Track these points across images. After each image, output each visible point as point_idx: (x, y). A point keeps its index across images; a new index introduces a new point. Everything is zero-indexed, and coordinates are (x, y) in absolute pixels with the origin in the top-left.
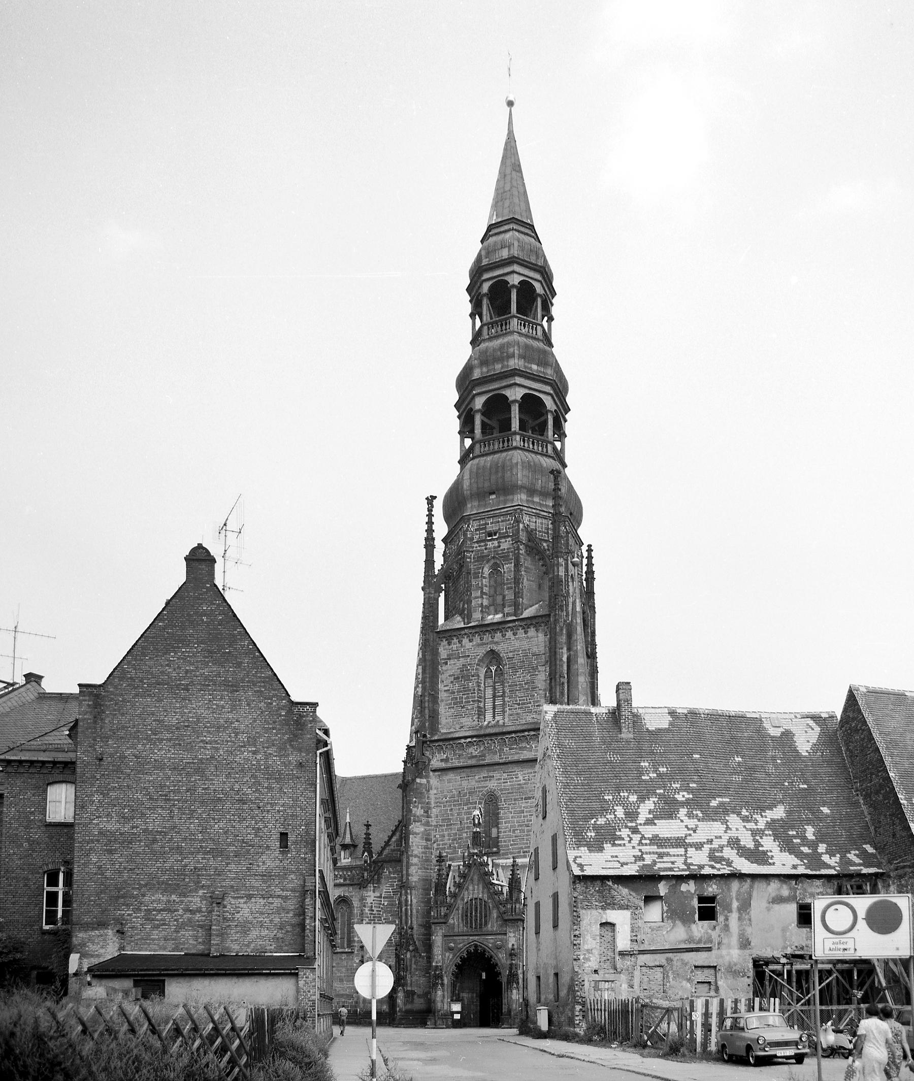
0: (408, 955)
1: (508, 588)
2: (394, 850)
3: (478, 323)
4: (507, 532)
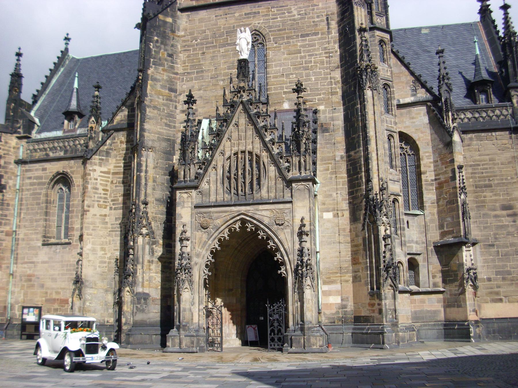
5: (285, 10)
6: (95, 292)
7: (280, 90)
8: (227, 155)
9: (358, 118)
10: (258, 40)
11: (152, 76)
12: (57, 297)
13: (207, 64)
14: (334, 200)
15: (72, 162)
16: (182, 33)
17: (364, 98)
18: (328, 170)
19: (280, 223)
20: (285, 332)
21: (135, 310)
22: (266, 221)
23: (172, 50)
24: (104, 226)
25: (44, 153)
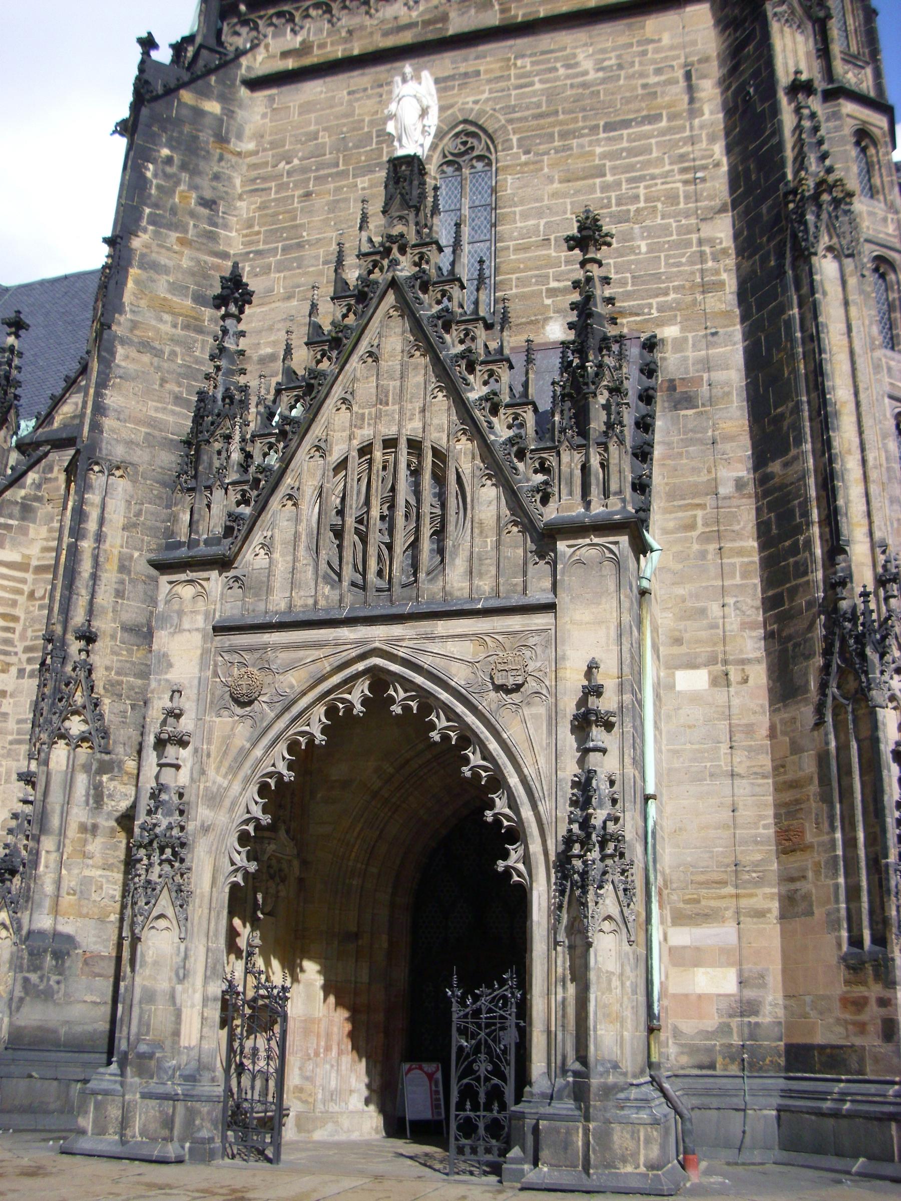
5: (557, 60)
7: (537, 283)
8: (335, 456)
9: (792, 348)
10: (472, 148)
11: (143, 255)
14: (714, 626)
16: (251, 146)
17: (812, 282)
18: (692, 527)
19: (510, 682)
20: (518, 1101)
21: (18, 993)
22: (459, 676)
23: (214, 188)
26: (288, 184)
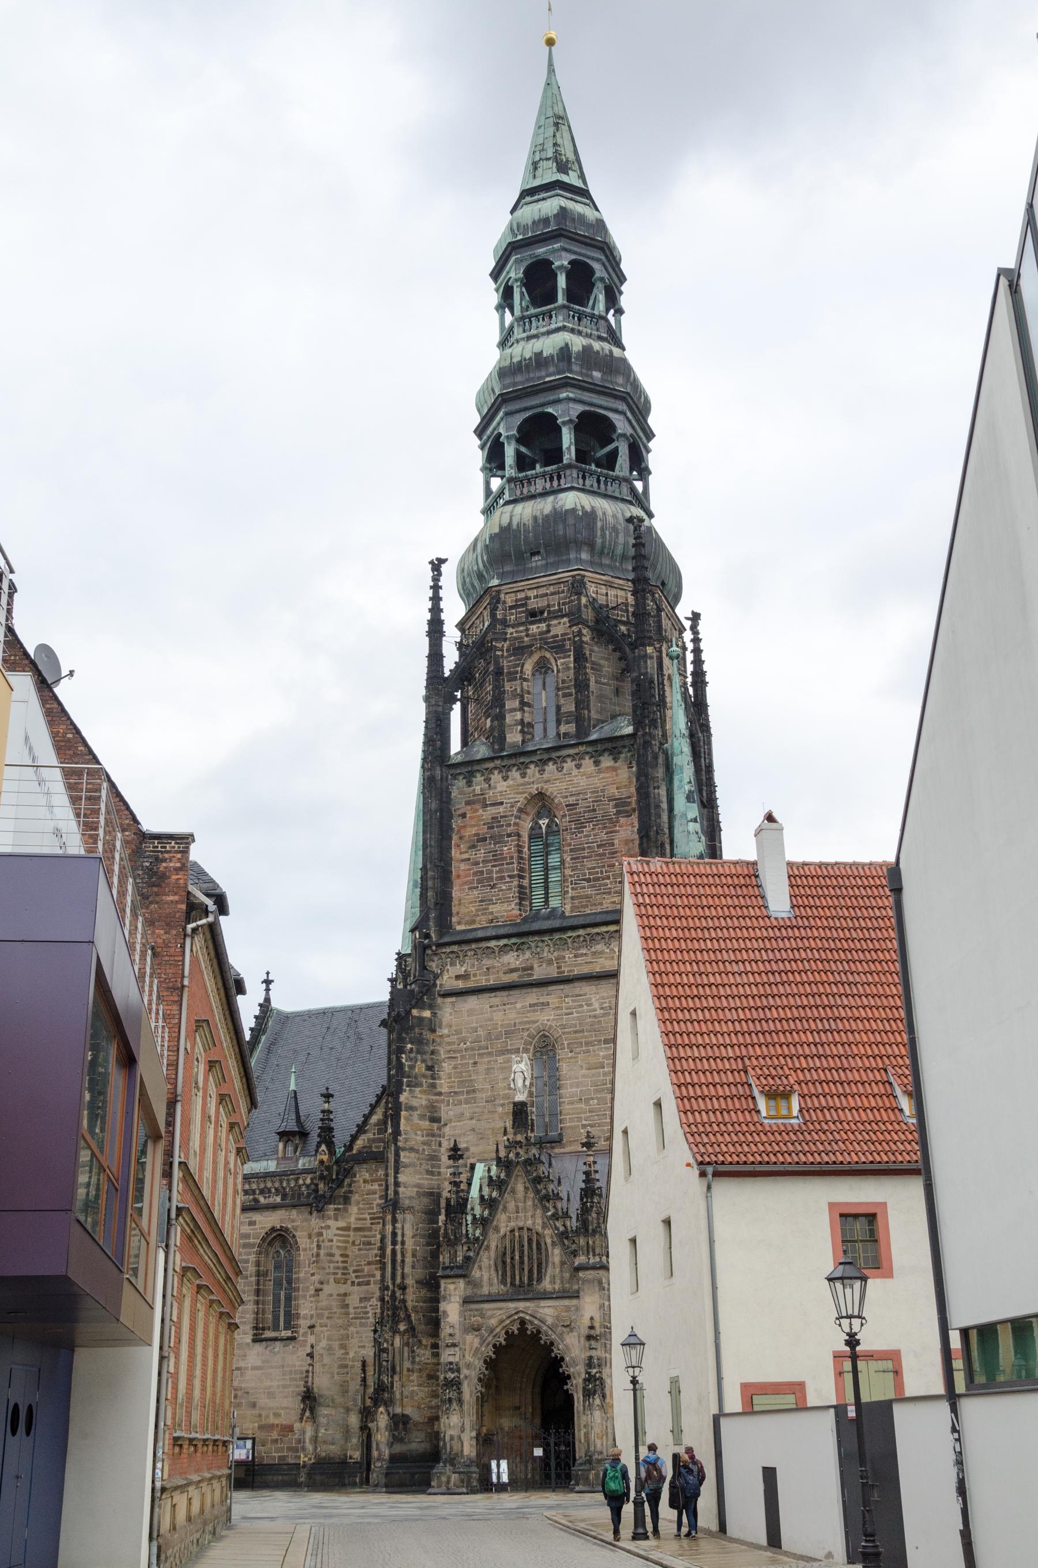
0: (397, 1341)
1: (565, 695)
2: (374, 1140)
3: (509, 318)
4: (560, 610)
6: (333, 1413)
7: (578, 1121)
8: (502, 1233)
11: (406, 1104)
12: (276, 1422)
13: (480, 1082)
15: (294, 1212)
21: (391, 1440)
22: (550, 1321)
24: (343, 1310)
25: (251, 1197)
26: (465, 1055)
